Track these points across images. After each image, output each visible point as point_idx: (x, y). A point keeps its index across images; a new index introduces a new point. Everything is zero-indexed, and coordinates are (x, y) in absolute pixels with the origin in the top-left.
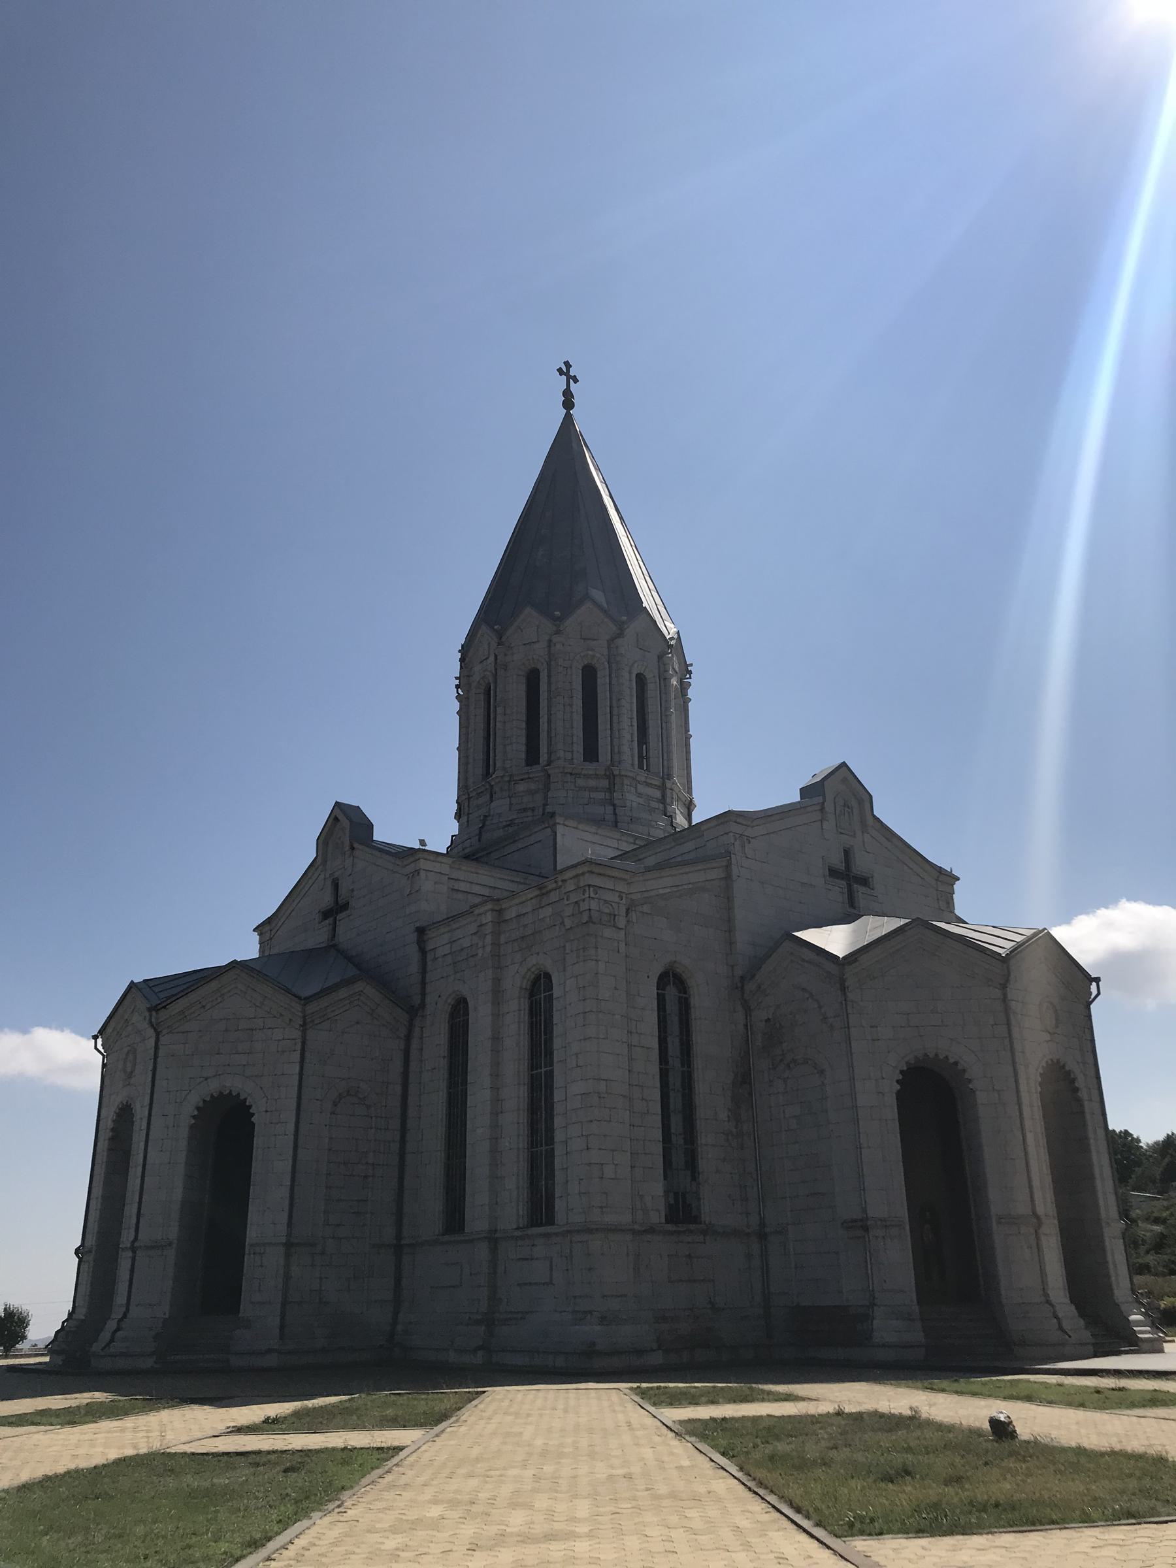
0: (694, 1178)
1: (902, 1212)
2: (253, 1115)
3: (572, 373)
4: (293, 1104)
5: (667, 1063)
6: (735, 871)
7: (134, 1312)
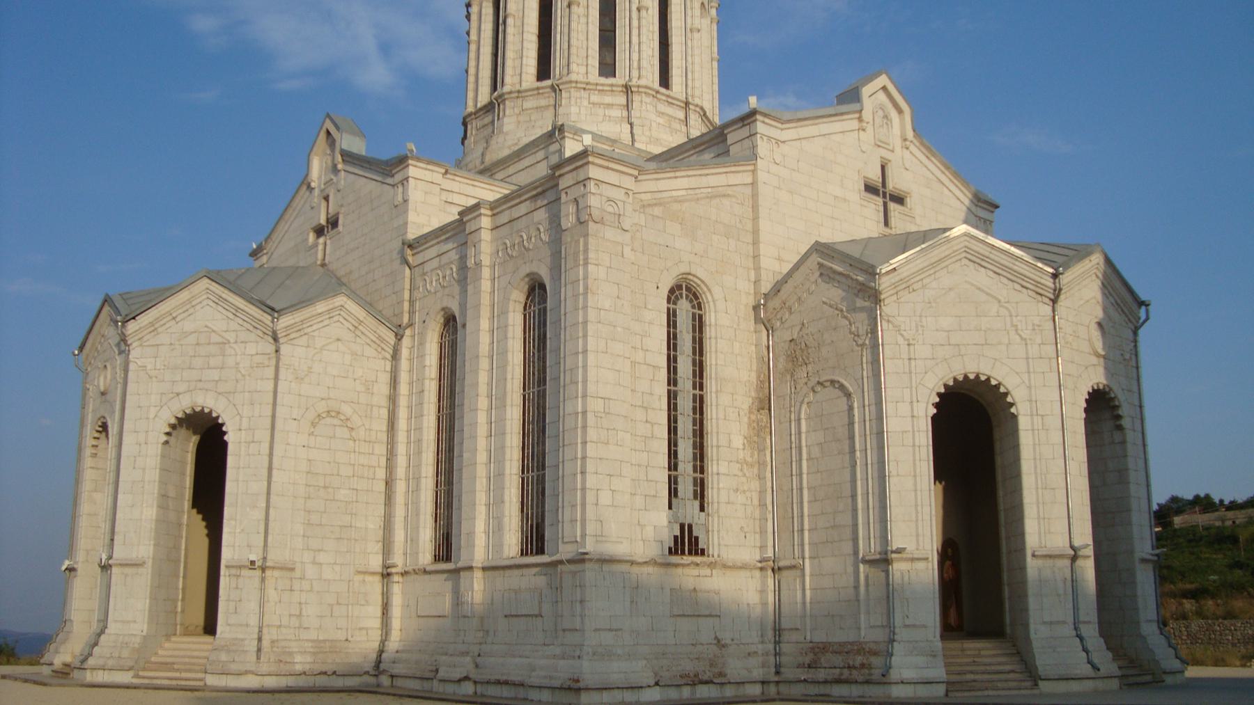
0: (702, 509)
2: (225, 433)
5: (675, 384)
7: (112, 628)
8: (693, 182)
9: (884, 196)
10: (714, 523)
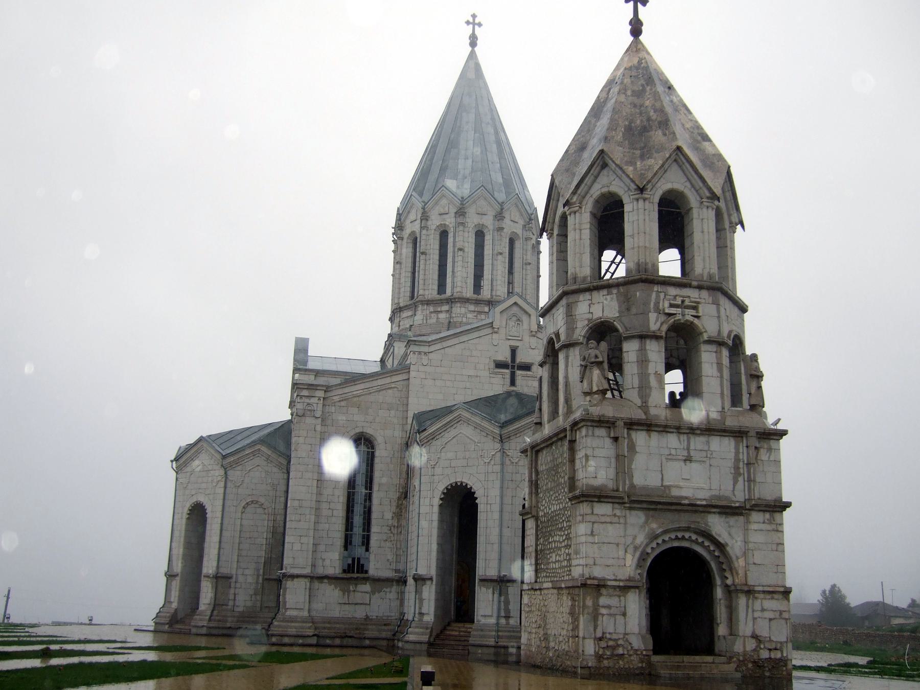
1: (433, 572)
3: (477, 21)
4: (220, 508)
6: (412, 374)
8: (367, 385)
9: (513, 367)
10: (372, 557)
